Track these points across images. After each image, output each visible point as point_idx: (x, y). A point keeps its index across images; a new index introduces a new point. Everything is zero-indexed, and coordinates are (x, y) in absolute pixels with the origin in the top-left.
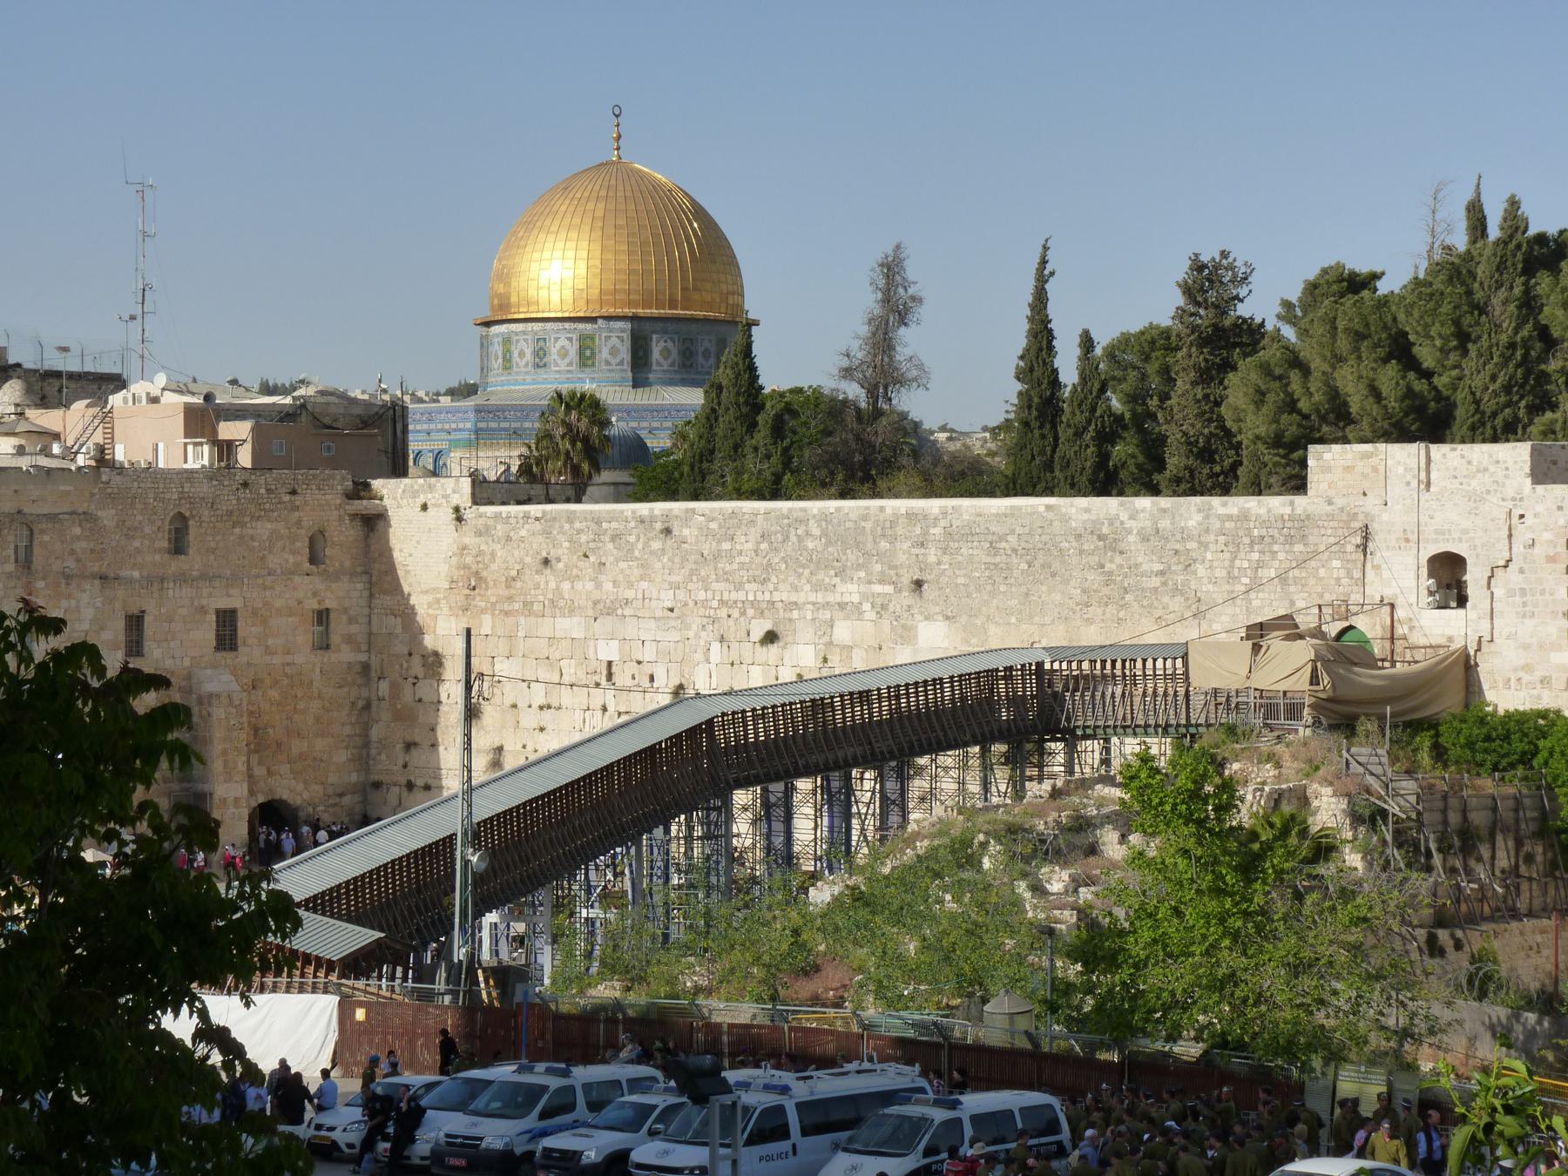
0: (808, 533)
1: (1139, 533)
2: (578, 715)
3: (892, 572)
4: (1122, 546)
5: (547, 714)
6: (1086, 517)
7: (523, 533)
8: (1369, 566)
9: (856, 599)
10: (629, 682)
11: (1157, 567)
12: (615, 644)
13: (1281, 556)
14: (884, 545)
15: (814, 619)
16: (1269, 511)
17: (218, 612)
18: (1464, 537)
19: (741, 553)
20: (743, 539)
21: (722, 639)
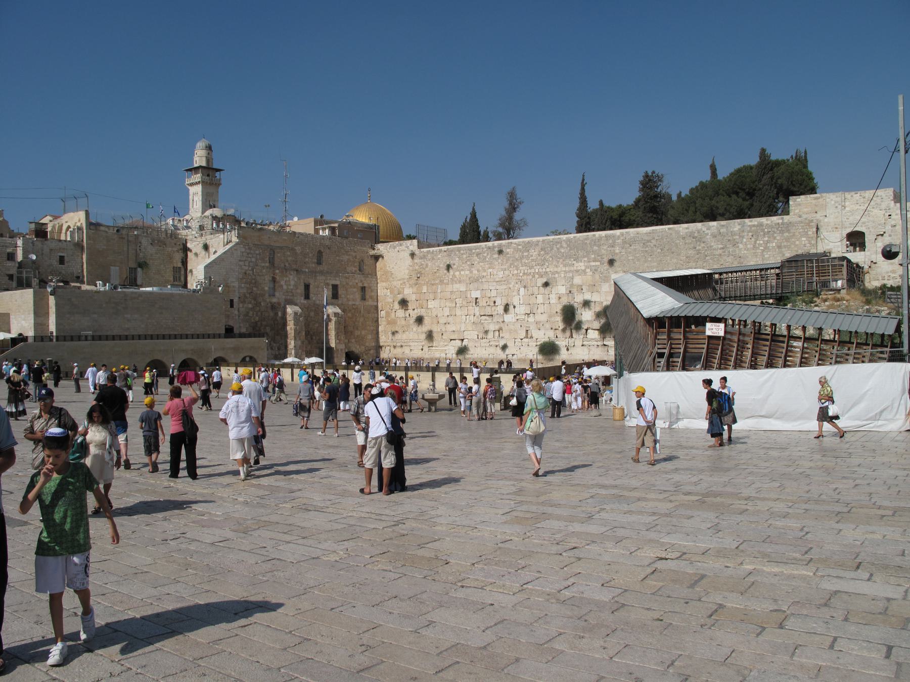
0: (562, 247)
1: (711, 235)
2: (464, 317)
4: (703, 240)
5: (450, 319)
6: (687, 231)
7: (439, 256)
9: (583, 268)
11: (720, 246)
12: (479, 292)
13: (778, 238)
14: (595, 248)
16: (772, 222)
18: (863, 225)
19: (532, 256)
20: (533, 251)
21: (525, 287)
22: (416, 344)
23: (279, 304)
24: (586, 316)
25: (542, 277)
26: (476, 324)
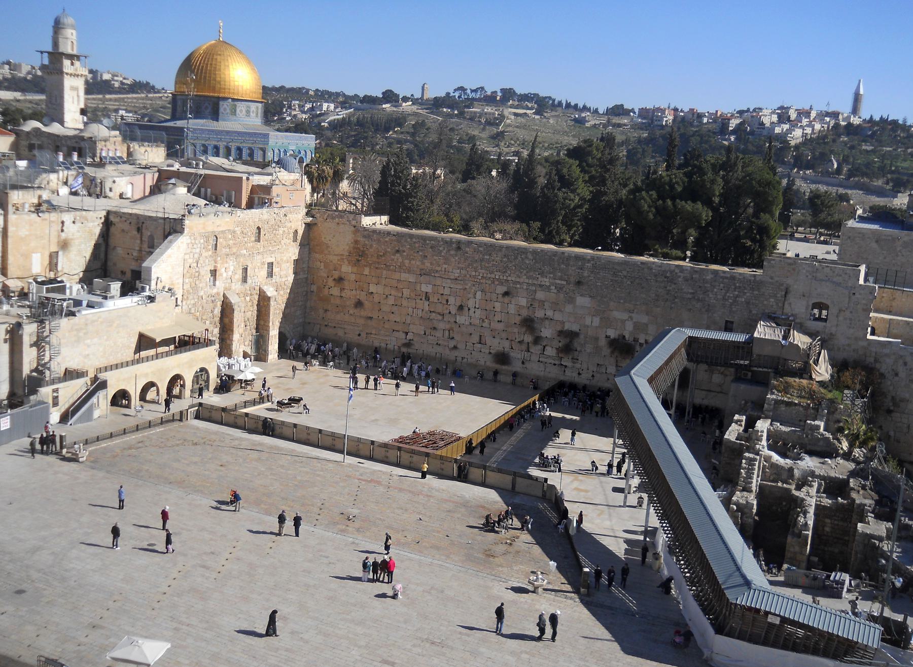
0: (527, 258)
2: (410, 310)
3: (566, 277)
5: (395, 309)
6: (660, 269)
7: (387, 239)
8: (786, 302)
9: (548, 284)
10: (436, 301)
11: (692, 291)
12: (430, 287)
13: (748, 294)
14: (563, 266)
15: (527, 289)
17: (271, 265)
19: (493, 260)
22: (352, 327)
23: (218, 294)
24: (547, 332)
25: (501, 284)
26: (424, 319)
